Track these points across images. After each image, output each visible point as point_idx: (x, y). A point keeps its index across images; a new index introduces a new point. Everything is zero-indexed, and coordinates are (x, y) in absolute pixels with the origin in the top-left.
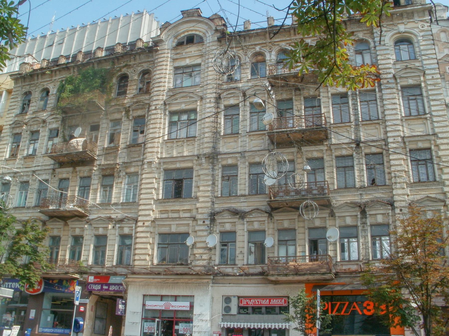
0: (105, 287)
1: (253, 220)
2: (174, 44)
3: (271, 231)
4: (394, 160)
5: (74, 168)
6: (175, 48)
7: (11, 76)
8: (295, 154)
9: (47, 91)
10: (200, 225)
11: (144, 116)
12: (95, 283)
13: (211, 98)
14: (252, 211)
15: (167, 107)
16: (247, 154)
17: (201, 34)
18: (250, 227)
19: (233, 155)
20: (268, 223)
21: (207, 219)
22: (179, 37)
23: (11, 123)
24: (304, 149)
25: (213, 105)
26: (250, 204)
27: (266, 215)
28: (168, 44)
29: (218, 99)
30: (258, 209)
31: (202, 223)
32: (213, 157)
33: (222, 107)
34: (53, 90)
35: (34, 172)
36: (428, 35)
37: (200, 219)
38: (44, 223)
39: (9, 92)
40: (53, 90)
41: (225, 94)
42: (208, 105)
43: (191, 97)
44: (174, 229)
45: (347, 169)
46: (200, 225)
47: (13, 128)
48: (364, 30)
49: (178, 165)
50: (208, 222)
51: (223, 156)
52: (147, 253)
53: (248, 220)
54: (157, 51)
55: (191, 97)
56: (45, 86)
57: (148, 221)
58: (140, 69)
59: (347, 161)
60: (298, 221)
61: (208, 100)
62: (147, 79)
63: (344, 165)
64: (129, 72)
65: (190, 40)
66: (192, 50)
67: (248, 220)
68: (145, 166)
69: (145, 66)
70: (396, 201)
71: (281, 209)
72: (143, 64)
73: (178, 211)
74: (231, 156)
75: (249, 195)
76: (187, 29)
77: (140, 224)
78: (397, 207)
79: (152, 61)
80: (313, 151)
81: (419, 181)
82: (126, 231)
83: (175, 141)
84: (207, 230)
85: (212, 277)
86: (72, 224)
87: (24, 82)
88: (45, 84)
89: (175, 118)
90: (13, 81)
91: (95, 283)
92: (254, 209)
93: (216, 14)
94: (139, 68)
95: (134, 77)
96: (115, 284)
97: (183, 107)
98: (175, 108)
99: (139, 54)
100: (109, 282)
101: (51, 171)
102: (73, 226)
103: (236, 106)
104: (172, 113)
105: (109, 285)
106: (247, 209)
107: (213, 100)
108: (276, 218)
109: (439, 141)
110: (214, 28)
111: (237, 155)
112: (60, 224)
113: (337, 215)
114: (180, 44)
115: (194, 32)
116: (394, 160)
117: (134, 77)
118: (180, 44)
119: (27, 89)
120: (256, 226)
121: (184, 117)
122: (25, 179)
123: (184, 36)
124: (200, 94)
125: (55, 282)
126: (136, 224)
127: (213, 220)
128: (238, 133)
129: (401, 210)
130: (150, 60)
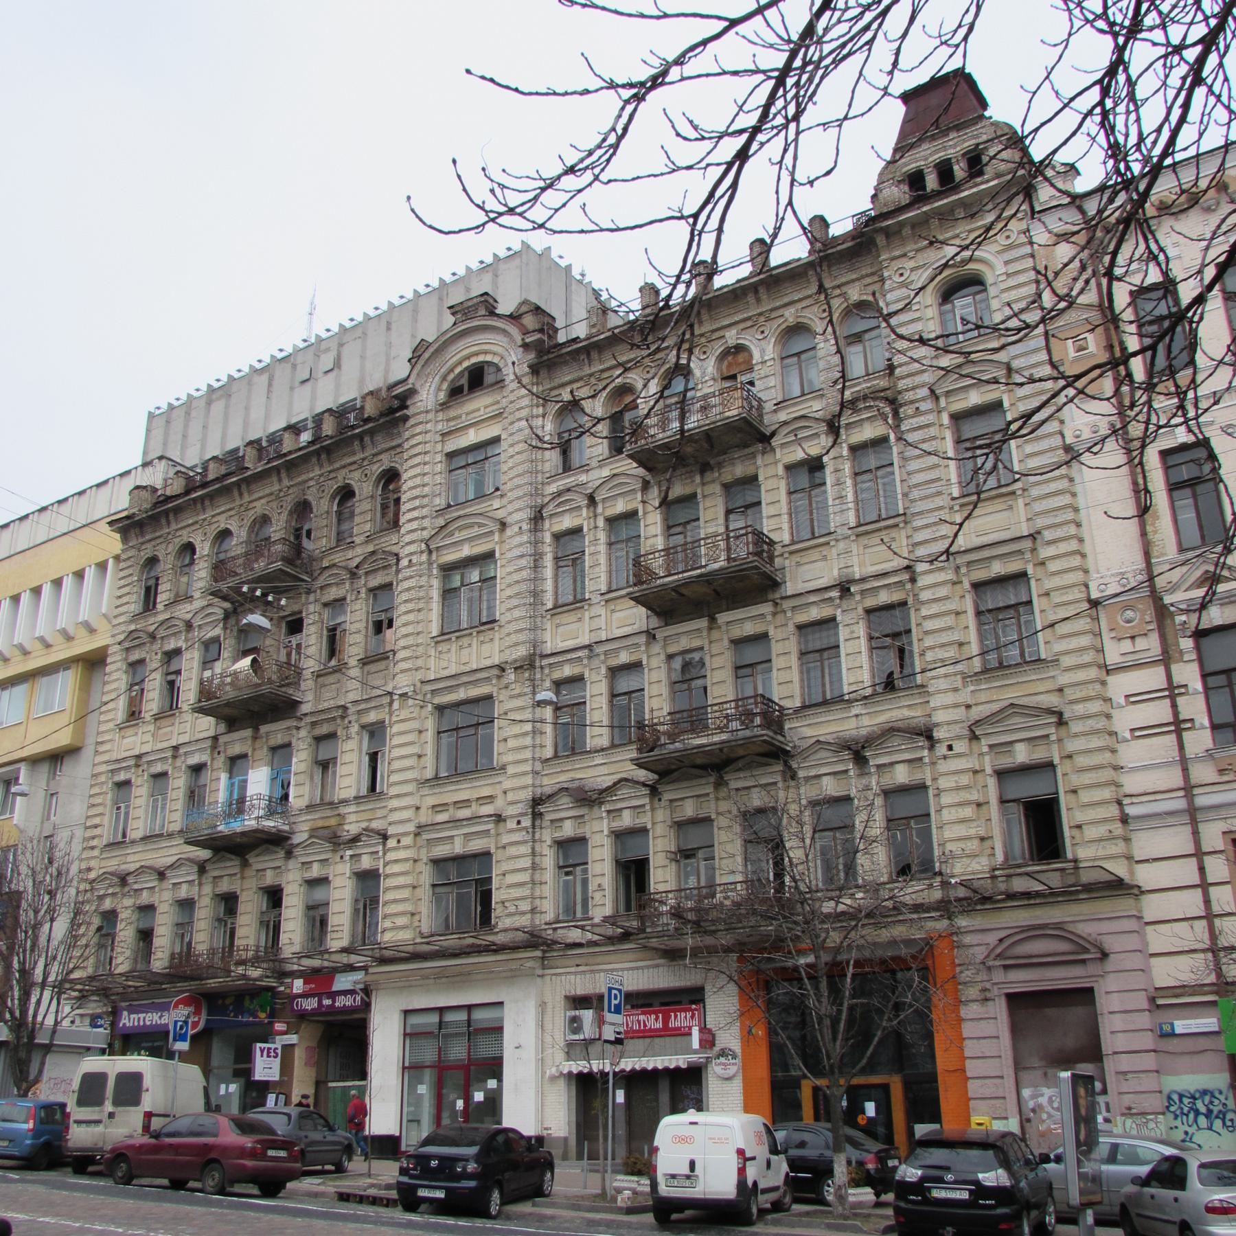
0: (327, 1002)
1: (619, 805)
2: (442, 396)
3: (660, 830)
4: (931, 617)
5: (256, 729)
6: (444, 406)
7: (111, 523)
8: (705, 633)
9: (189, 548)
10: (512, 831)
11: (391, 584)
12: (304, 995)
13: (521, 521)
14: (615, 784)
15: (434, 557)
16: (599, 649)
17: (496, 360)
18: (614, 824)
19: (574, 655)
20: (653, 809)
21: (525, 814)
22: (451, 376)
23: (122, 637)
24: (722, 618)
25: (525, 538)
26: (613, 768)
27: (646, 791)
28: (429, 394)
29: (538, 518)
30: (626, 780)
31: (514, 826)
32: (528, 665)
33: (548, 538)
34: (204, 548)
35: (176, 748)
36: (1023, 257)
37: (512, 817)
38: (202, 868)
39: (117, 558)
40: (204, 548)
41: (551, 506)
42: (517, 540)
43: (480, 525)
44: (458, 848)
45: (826, 654)
46: (512, 831)
47: (128, 649)
48: (863, 277)
49: (462, 694)
50: (527, 822)
51: (552, 660)
52: (408, 913)
53: (609, 807)
54: (406, 419)
55: (480, 525)
56: (185, 540)
57: (406, 834)
58: (377, 469)
59: (824, 634)
60: (717, 799)
61: (516, 529)
62: (394, 491)
63: (818, 646)
64: (354, 479)
65: (476, 379)
66: (480, 404)
67: (609, 807)
68: (396, 705)
69: (385, 462)
70: (937, 725)
71: (676, 774)
72: (382, 457)
73: (466, 803)
74: (569, 656)
75: (613, 746)
76: (463, 354)
77: (391, 843)
78: (939, 741)
79: (399, 446)
80: (743, 621)
81: (1001, 663)
82: (366, 863)
83: (453, 636)
84: (525, 842)
85: (538, 953)
86: (258, 861)
87: (142, 534)
88: (184, 532)
89: (456, 581)
90: (118, 536)
91: (304, 995)
92: (620, 781)
93: (525, 302)
94: (375, 467)
95: (365, 488)
96: (345, 993)
97: (466, 551)
98: (451, 557)
99: (371, 432)
100: (335, 988)
101: (209, 743)
102: (260, 866)
103: (577, 531)
104: (448, 569)
105: (333, 995)
106: (607, 782)
107: (525, 527)
108: (667, 796)
109: (1045, 552)
110: (520, 342)
111: (580, 654)
112: (232, 865)
113: (801, 774)
114: (456, 392)
115: (481, 358)
116: (931, 617)
117: (365, 488)
118: (456, 392)
119: (147, 552)
120: (627, 820)
121: (474, 575)
122: (158, 768)
123: (462, 372)
124: (500, 514)
125: (228, 1001)
126: (384, 844)
127: (537, 816)
128: (584, 600)
129: (950, 748)
130: (394, 443)
